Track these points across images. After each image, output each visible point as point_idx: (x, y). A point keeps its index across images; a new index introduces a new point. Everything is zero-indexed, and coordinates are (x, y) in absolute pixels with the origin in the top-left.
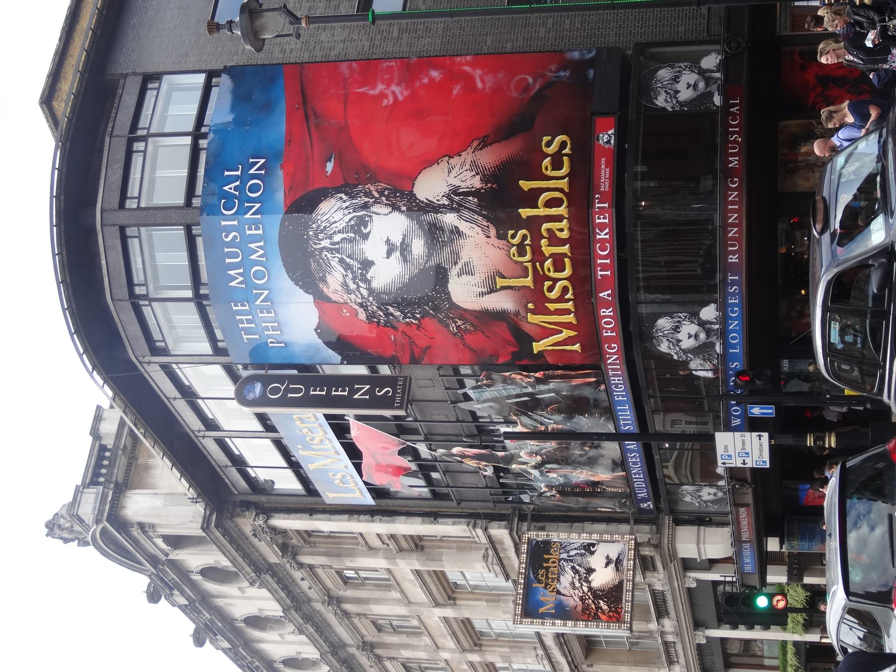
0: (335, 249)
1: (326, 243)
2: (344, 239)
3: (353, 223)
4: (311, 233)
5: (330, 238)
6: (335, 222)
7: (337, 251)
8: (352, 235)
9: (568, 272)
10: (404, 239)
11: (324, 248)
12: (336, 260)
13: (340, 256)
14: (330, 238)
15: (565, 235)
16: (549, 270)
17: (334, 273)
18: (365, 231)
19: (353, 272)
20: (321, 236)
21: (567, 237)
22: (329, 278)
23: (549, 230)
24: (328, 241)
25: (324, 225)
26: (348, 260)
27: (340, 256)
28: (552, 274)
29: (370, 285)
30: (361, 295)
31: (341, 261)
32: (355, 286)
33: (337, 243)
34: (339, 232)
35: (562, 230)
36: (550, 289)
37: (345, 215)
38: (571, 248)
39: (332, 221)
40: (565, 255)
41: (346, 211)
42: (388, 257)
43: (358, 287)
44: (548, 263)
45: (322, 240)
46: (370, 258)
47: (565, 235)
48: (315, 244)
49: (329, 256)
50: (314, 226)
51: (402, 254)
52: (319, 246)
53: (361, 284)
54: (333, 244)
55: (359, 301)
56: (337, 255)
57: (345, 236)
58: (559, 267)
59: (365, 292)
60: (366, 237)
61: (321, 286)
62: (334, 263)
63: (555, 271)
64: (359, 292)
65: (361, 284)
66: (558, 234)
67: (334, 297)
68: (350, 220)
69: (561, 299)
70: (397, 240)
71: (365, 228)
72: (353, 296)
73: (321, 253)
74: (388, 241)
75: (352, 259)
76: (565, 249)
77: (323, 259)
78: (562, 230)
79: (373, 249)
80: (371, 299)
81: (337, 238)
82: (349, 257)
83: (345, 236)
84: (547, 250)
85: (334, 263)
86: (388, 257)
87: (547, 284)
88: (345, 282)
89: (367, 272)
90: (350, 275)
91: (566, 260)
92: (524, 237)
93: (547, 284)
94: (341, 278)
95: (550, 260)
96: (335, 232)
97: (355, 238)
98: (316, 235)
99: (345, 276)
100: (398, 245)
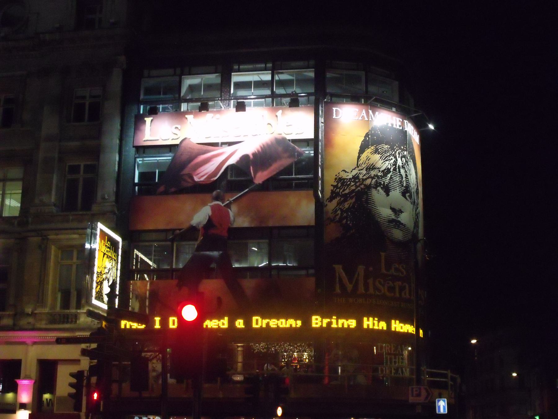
0: (396, 166)
1: (399, 162)
4: (405, 153)
7: (395, 169)
10: (402, 224)
11: (397, 160)
13: (391, 170)
24: (401, 165)
26: (389, 176)
27: (391, 170)
29: (374, 188)
30: (366, 179)
32: (373, 176)
33: (400, 172)
46: (390, 193)
48: (399, 154)
49: (392, 161)
52: (397, 156)
53: (374, 180)
55: (361, 177)
56: (392, 168)
59: (368, 182)
64: (368, 178)
65: (374, 180)
72: (364, 172)
74: (402, 212)
80: (362, 186)
82: (391, 178)
85: (387, 165)
88: (375, 168)
89: (382, 188)
90: (380, 174)
96: (406, 172)
100: (399, 219)
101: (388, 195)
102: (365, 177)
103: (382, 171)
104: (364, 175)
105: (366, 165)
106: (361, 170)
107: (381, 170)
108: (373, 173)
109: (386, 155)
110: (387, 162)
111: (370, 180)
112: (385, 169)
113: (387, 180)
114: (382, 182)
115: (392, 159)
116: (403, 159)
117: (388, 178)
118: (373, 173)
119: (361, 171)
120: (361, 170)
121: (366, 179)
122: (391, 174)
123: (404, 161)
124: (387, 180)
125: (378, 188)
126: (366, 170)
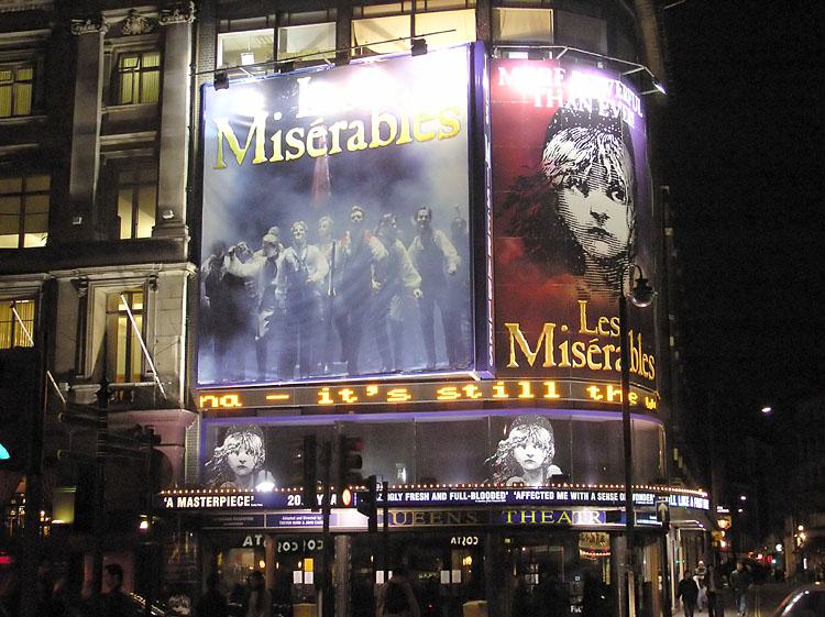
1: (602, 151)
3: (621, 183)
7: (595, 160)
9: (593, 366)
10: (608, 234)
12: (588, 157)
16: (593, 349)
18: (614, 194)
22: (570, 144)
24: (604, 154)
26: (588, 169)
28: (590, 351)
30: (555, 176)
33: (602, 162)
34: (612, 167)
36: (579, 348)
38: (608, 371)
42: (592, 213)
44: (598, 349)
49: (591, 150)
51: (595, 229)
52: (599, 141)
53: (567, 177)
57: (609, 172)
60: (609, 194)
64: (559, 174)
65: (567, 177)
69: (572, 356)
70: (608, 226)
71: (617, 196)
76: (608, 366)
81: (607, 163)
82: (591, 172)
85: (584, 155)
86: (592, 213)
87: (583, 345)
90: (574, 168)
91: (600, 365)
100: (603, 227)
101: (586, 195)
108: (565, 167)
109: (583, 141)
113: (584, 176)
118: (565, 167)
121: (555, 176)
122: (590, 166)
124: (584, 176)
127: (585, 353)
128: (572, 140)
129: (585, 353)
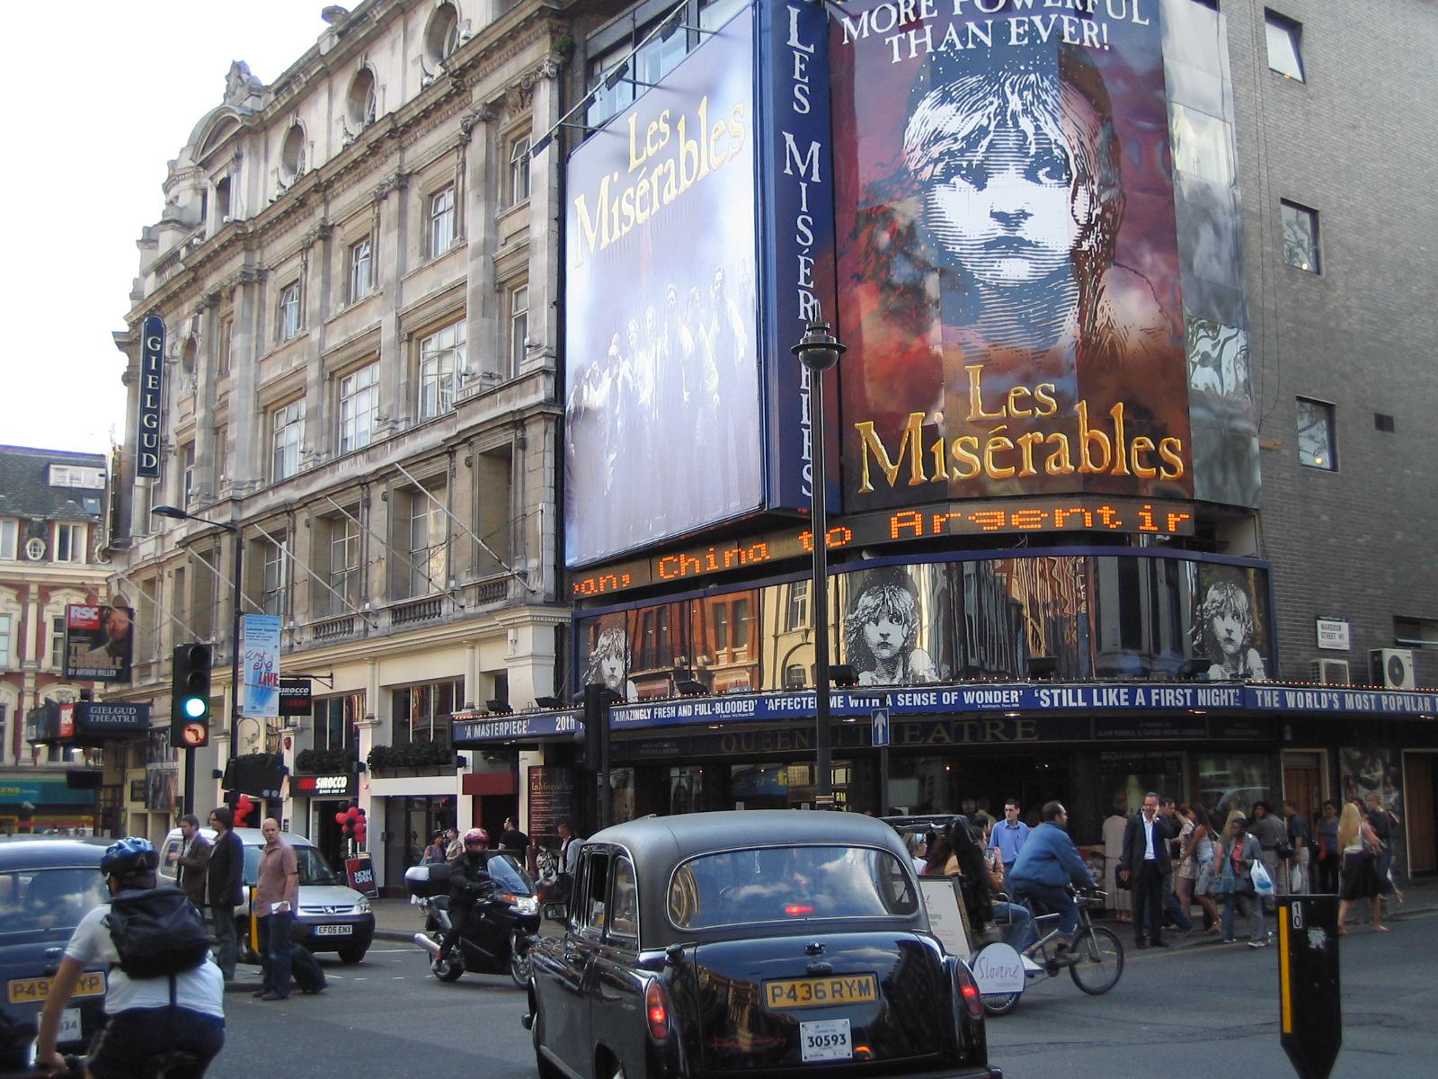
1: (1015, 103)
2: (1026, 137)
3: (1057, 152)
4: (1032, 77)
5: (1025, 112)
6: (1055, 120)
7: (1002, 124)
8: (1033, 151)
11: (1006, 101)
12: (985, 122)
13: (992, 128)
14: (1025, 112)
15: (1051, 467)
17: (959, 118)
19: (962, 151)
20: (1028, 95)
21: (1048, 469)
22: (949, 109)
23: (1057, 444)
24: (1019, 108)
25: (1050, 100)
26: (985, 143)
27: (992, 128)
29: (940, 182)
30: (922, 169)
31: (982, 131)
33: (1016, 124)
34: (1038, 128)
35: (1058, 463)
37: (1069, 139)
39: (1058, 115)
40: (1019, 467)
41: (1075, 142)
43: (936, 161)
45: (1021, 97)
46: (990, 182)
47: (1051, 467)
48: (1013, 86)
49: (992, 109)
50: (1046, 83)
52: (1008, 90)
53: (941, 165)
54: (1014, 115)
56: (993, 124)
57: (1031, 137)
58: (1002, 458)
59: (926, 174)
60: (1031, 175)
61: (933, 94)
62: (978, 119)
63: (995, 453)
64: (927, 164)
65: (941, 165)
66: (1052, 457)
67: (915, 121)
68: (1064, 151)
72: (918, 153)
73: (996, 94)
75: (988, 150)
77: (984, 98)
78: (1058, 463)
79: (1009, 189)
81: (1026, 124)
83: (1031, 137)
84: (1027, 441)
85: (978, 119)
87: (975, 441)
88: (943, 138)
89: (963, 177)
90: (956, 147)
92: (1045, 407)
93: (975, 441)
94: (948, 130)
95: (1012, 446)
96: (1036, 119)
97: (1027, 155)
98: (1028, 87)
99: (954, 137)
102: (920, 165)
103: (963, 139)
104: (919, 161)
105: (920, 137)
106: (912, 151)
107: (960, 136)
110: (980, 113)
111: (931, 166)
112: (973, 132)
113: (978, 156)
114: (965, 164)
115: (991, 103)
116: (1025, 93)
117: (984, 149)
118: (935, 151)
119: (912, 155)
120: (912, 151)
123: (1030, 97)
124: (978, 156)
125: (952, 181)
126: (922, 149)
127: (980, 453)
128: (951, 102)
129: (980, 453)
